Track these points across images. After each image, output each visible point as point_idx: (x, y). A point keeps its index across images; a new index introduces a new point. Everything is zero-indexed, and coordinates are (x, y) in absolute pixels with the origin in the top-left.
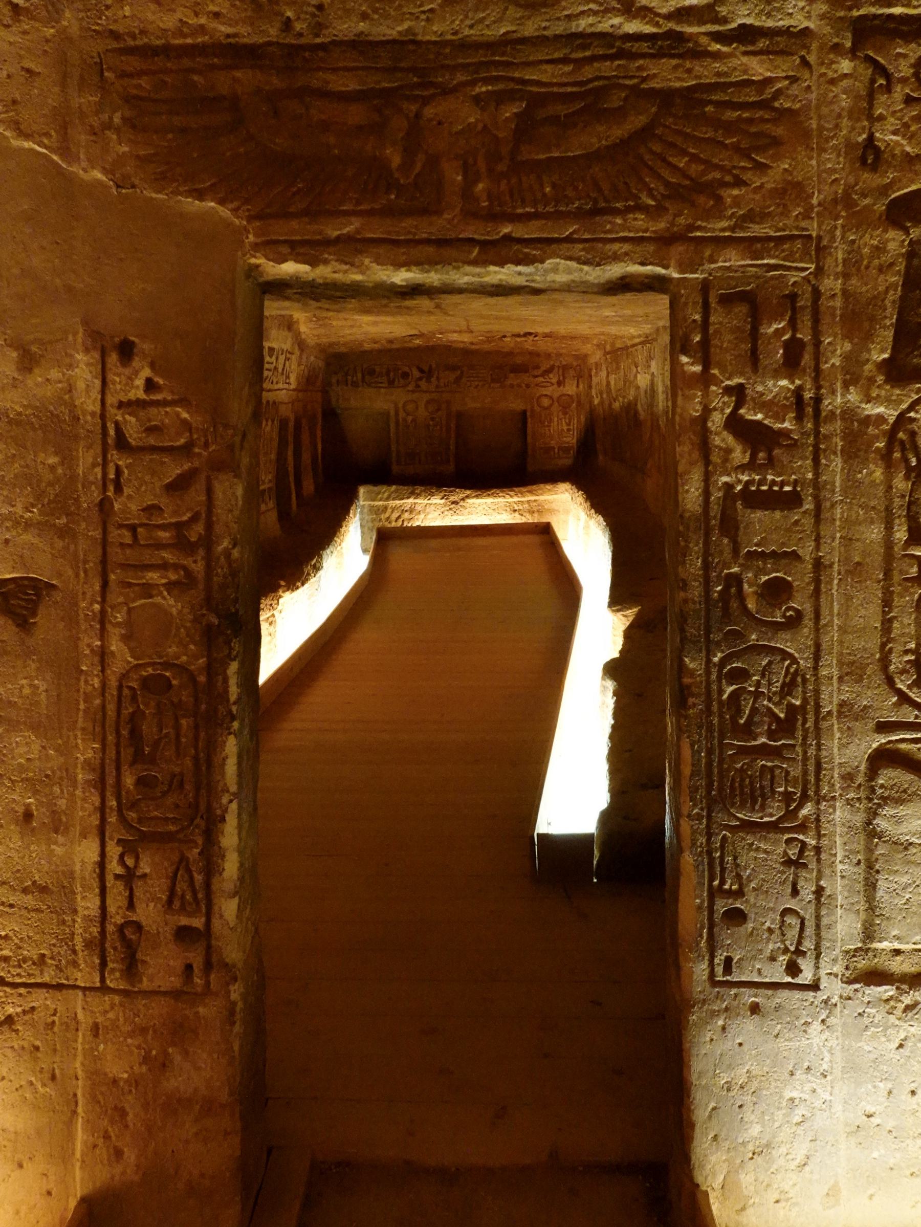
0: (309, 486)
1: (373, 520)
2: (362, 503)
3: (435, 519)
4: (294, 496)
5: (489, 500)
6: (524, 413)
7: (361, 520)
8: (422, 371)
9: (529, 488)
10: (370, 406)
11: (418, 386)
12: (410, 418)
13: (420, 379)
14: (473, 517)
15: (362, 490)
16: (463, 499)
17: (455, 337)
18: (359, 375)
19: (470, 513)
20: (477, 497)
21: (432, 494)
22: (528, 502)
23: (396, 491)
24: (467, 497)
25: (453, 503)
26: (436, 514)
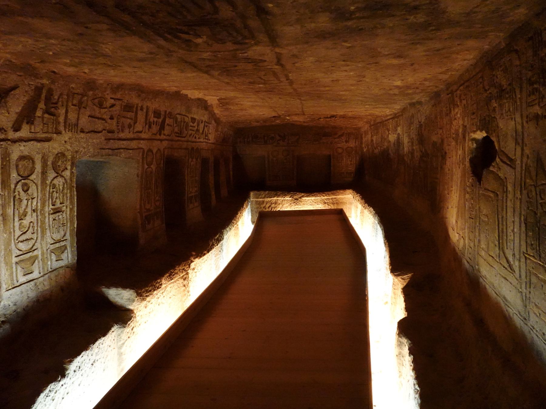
0: (224, 192)
1: (257, 208)
2: (252, 200)
3: (287, 207)
4: (213, 197)
5: (313, 198)
6: (330, 156)
7: (251, 208)
8: (280, 136)
9: (332, 192)
10: (255, 153)
11: (278, 144)
12: (275, 159)
13: (279, 140)
14: (305, 206)
15: (252, 194)
16: (300, 198)
17: (296, 118)
18: (250, 138)
19: (303, 204)
20: (307, 196)
21: (285, 195)
22: (332, 199)
23: (268, 194)
24: (303, 196)
25: (296, 199)
26: (288, 205)
